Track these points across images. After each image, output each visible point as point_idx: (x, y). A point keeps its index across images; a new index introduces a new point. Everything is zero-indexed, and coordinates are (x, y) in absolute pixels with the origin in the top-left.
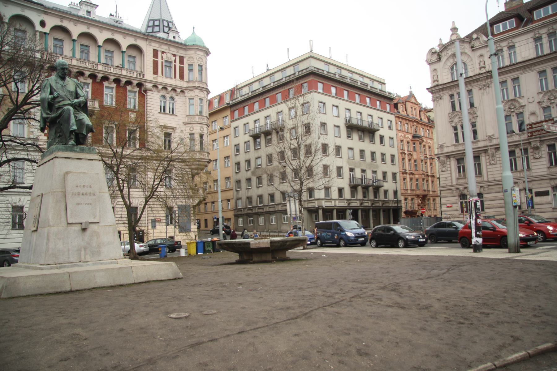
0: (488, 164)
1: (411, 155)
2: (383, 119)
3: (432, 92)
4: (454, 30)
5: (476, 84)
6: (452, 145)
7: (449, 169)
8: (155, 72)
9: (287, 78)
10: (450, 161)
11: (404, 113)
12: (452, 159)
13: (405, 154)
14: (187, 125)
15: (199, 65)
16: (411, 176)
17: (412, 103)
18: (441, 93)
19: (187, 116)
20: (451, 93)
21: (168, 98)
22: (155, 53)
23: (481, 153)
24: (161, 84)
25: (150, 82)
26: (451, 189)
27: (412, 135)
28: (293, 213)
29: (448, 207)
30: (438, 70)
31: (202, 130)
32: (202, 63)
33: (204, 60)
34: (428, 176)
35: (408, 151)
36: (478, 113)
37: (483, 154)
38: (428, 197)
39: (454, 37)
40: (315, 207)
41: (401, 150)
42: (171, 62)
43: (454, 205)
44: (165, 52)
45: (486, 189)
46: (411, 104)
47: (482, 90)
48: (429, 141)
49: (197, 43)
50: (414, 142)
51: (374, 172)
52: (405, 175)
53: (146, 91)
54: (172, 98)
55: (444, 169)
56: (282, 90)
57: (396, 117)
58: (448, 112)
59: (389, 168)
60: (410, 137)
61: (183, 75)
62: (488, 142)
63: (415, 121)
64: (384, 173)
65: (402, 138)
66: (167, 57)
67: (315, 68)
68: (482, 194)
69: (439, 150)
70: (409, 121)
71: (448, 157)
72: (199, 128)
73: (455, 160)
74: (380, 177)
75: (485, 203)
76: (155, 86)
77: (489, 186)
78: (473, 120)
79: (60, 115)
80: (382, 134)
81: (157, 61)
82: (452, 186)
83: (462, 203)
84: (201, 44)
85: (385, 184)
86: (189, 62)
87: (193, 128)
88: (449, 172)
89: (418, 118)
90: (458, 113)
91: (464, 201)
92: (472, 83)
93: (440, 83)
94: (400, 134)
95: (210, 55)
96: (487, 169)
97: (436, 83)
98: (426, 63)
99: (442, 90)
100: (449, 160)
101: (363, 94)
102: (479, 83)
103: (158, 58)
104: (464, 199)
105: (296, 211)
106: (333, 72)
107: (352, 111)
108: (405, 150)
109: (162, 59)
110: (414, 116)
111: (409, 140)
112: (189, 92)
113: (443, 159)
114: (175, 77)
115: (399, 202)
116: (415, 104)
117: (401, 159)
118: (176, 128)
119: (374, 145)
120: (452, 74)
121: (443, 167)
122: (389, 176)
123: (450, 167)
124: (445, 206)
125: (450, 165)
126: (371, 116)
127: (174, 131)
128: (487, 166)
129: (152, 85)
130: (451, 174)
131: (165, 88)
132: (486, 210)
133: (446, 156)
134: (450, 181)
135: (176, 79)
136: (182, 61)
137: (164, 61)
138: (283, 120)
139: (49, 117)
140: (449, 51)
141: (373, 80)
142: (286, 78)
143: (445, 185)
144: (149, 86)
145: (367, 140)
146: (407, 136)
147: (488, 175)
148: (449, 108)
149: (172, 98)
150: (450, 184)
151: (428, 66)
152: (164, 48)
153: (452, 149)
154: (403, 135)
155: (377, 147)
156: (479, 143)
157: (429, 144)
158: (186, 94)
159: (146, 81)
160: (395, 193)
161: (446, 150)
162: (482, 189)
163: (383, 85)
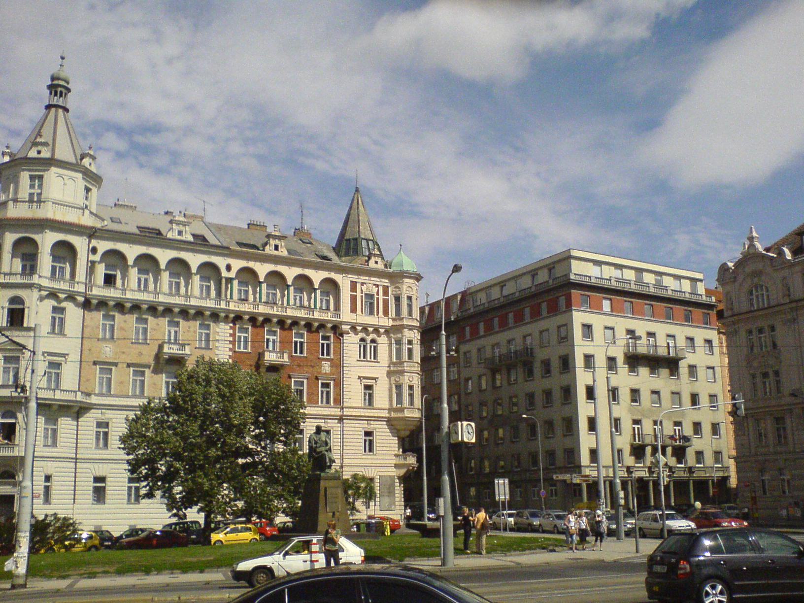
8: (353, 310)
25: (347, 323)
31: (411, 379)
44: (365, 283)
53: (342, 335)
74: (688, 431)
86: (394, 293)
118: (378, 378)
127: (376, 382)
129: (349, 327)
131: (365, 329)
135: (379, 316)
137: (364, 295)
144: (345, 328)
152: (364, 279)
159: (341, 323)
160: (718, 455)
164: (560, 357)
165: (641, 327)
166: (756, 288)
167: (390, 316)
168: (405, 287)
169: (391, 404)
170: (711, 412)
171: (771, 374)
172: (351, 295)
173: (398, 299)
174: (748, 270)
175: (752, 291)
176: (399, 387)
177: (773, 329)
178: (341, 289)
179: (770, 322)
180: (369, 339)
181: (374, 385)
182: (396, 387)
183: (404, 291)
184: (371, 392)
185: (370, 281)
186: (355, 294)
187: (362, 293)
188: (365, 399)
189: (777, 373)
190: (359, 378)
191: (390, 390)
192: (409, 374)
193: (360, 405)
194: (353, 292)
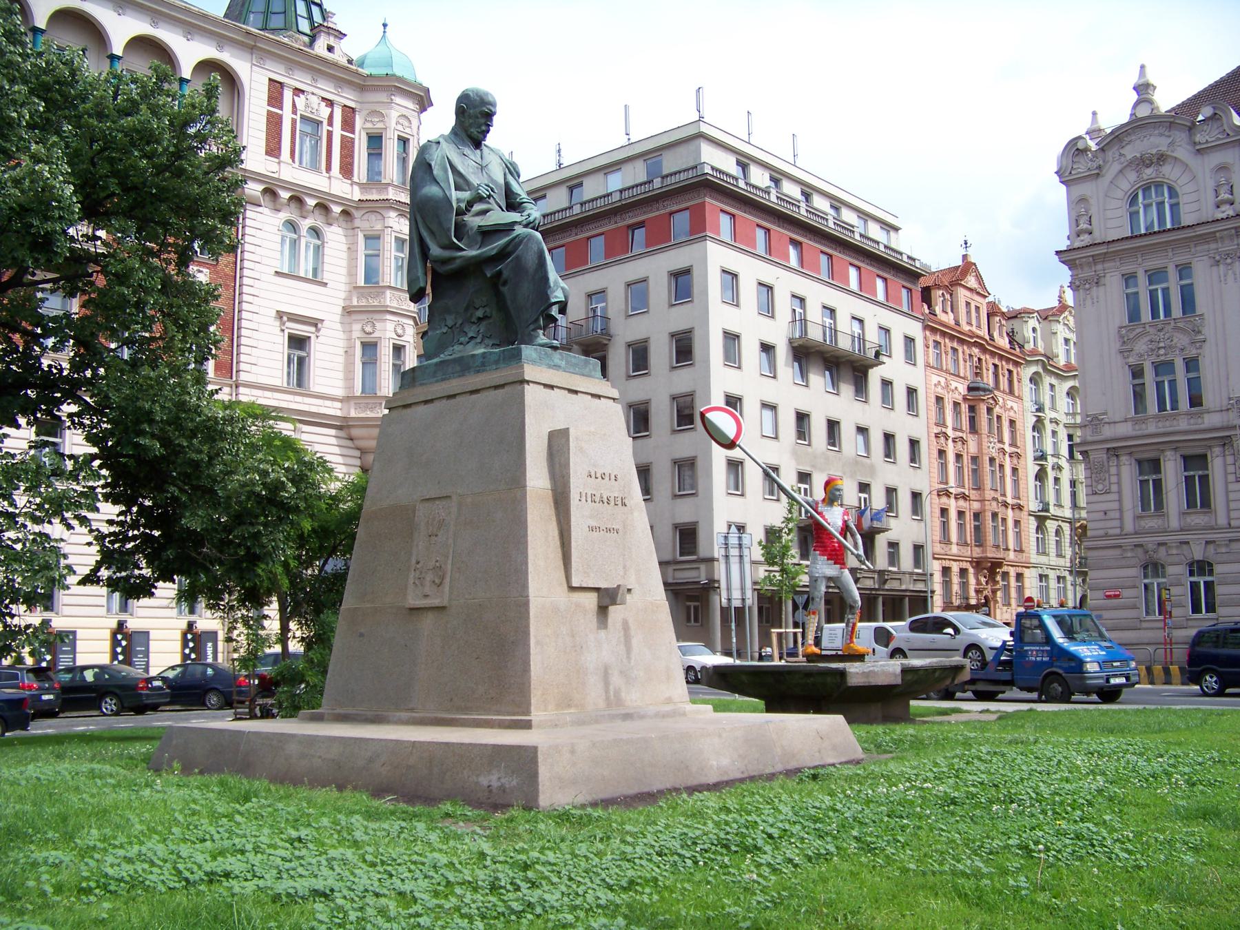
0: (1231, 478)
1: (964, 441)
2: (892, 332)
3: (1070, 264)
4: (1143, 90)
5: (1206, 247)
6: (1126, 421)
7: (1114, 488)
8: (273, 149)
9: (626, 194)
10: (1118, 466)
11: (949, 319)
12: (1124, 459)
13: (946, 437)
14: (354, 317)
15: (400, 138)
16: (961, 503)
17: (970, 290)
18: (1099, 267)
19: (355, 288)
20: (1128, 269)
21: (304, 231)
22: (276, 91)
23: (1163, 451)
24: (287, 186)
25: (258, 177)
26: (1121, 547)
27: (967, 383)
28: (736, 594)
29: (1109, 597)
30: (1093, 201)
31: (400, 332)
32: (408, 130)
33: (415, 123)
34: (1005, 505)
35: (954, 429)
36: (1208, 332)
37: (1217, 450)
38: (1005, 569)
39: (1143, 112)
40: (698, 583)
41: (937, 425)
42: (319, 123)
43: (1125, 593)
44: (303, 92)
45: (1224, 550)
46: (968, 293)
47: (1222, 267)
48: (1010, 404)
49: (398, 72)
50: (972, 403)
51: (864, 487)
52: (944, 499)
54: (315, 231)
55: (1100, 487)
56: (608, 227)
57: (926, 327)
58: (1117, 324)
59: (903, 476)
60: (962, 388)
61: (352, 164)
63: (976, 344)
64: (891, 492)
65: (939, 390)
66: (307, 106)
67: (713, 168)
68: (1210, 565)
69: (1088, 431)
70: (962, 341)
71: (1114, 453)
72: (390, 326)
73: (1133, 461)
75: (1219, 590)
76: (270, 192)
78: (1193, 352)
79: (503, 254)
80: (888, 376)
81: (280, 117)
82: (1122, 535)
83: (1194, 587)
84: (408, 76)
85: (893, 523)
86: (369, 125)
87: (374, 326)
88: (1115, 497)
89: (984, 332)
90: (1148, 329)
91: (1201, 581)
92: (1192, 245)
93: (1098, 237)
94: (935, 379)
95: (430, 109)
96: (1227, 492)
97: (1086, 240)
98: (1057, 178)
99: (1105, 257)
100: (1114, 461)
101: (840, 255)
102: (1213, 246)
103: (281, 109)
104: (1156, 575)
105: (743, 589)
106: (763, 186)
107: (808, 303)
108: (946, 427)
109: (294, 111)
110: (974, 329)
111: (959, 399)
112: (366, 217)
113: (1098, 456)
114: (329, 169)
115: (925, 577)
116: (978, 293)
117: (935, 454)
119: (866, 406)
120: (1134, 216)
121: (1097, 482)
122: (904, 501)
123: (1119, 483)
124: (1100, 594)
125: (1118, 475)
126: (861, 321)
127: (318, 330)
128: (1227, 483)
129: (261, 187)
130: (1120, 501)
132: (1221, 611)
133: (1108, 449)
134: (1117, 523)
136: (348, 124)
137: (298, 118)
138: (605, 319)
139: (454, 258)
140: (1128, 148)
141: (865, 216)
142: (621, 191)
143: (1101, 532)
145: (847, 390)
146: (954, 384)
147: (1229, 510)
148: (1119, 316)
149: (315, 231)
150: (1118, 531)
151: (1063, 188)
153: (1124, 429)
154: (943, 380)
155: (873, 414)
157: (1012, 414)
158: (357, 223)
161: (1107, 432)
162: (1211, 548)
163: (892, 233)
164: (673, 335)
165: (818, 294)
166: (1146, 189)
167: (355, 179)
168: (394, 114)
169: (350, 387)
170: (911, 469)
171: (1179, 365)
172: (268, 111)
173: (375, 141)
174: (1131, 152)
175: (1136, 195)
176: (370, 347)
177: (1184, 270)
178: (247, 96)
179: (1182, 258)
180: (306, 224)
181: (313, 337)
182: (365, 345)
183: (393, 124)
184: (303, 354)
185: (315, 91)
186: (279, 112)
187: (294, 112)
188: (289, 374)
189: (1192, 364)
190: (280, 315)
191: (348, 353)
192: (395, 318)
193: (278, 382)
194: (273, 106)
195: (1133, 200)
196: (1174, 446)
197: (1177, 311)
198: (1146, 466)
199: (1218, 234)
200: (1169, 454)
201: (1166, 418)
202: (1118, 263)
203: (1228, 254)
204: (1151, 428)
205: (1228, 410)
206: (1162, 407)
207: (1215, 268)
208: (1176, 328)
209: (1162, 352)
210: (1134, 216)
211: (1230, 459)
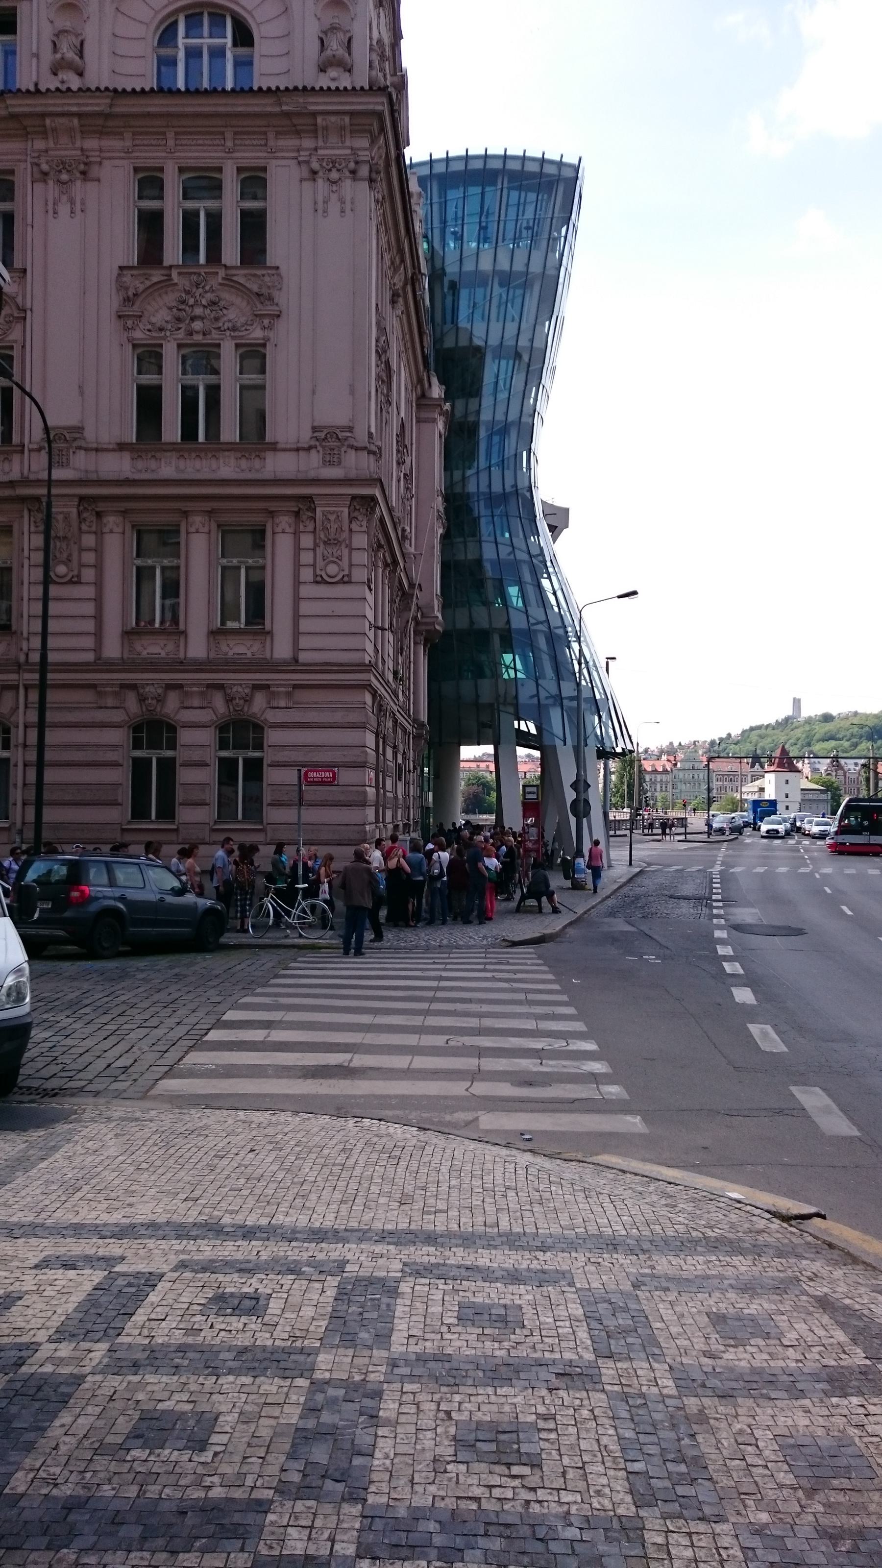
0: (307, 574)
7: (89, 575)
12: (111, 521)
18: (91, 143)
26: (94, 686)
37: (285, 522)
62: (315, 458)
68: (259, 728)
77: (295, 687)
78: (257, 334)
82: (101, 664)
96: (297, 599)
120: (167, 63)
123: (99, 567)
125: (98, 550)
128: (297, 583)
130: (98, 600)
150: (90, 657)
156: (269, 456)
175: (175, 24)
179: (250, 156)
195: (167, 35)
196: (208, 506)
197: (231, 252)
198: (150, 541)
199: (319, 120)
200: (197, 520)
201: (200, 452)
202: (128, 143)
203: (334, 162)
204: (168, 468)
205: (309, 448)
206: (189, 431)
207: (307, 185)
208: (230, 283)
209: (197, 325)
210: (167, 63)
211: (307, 541)
